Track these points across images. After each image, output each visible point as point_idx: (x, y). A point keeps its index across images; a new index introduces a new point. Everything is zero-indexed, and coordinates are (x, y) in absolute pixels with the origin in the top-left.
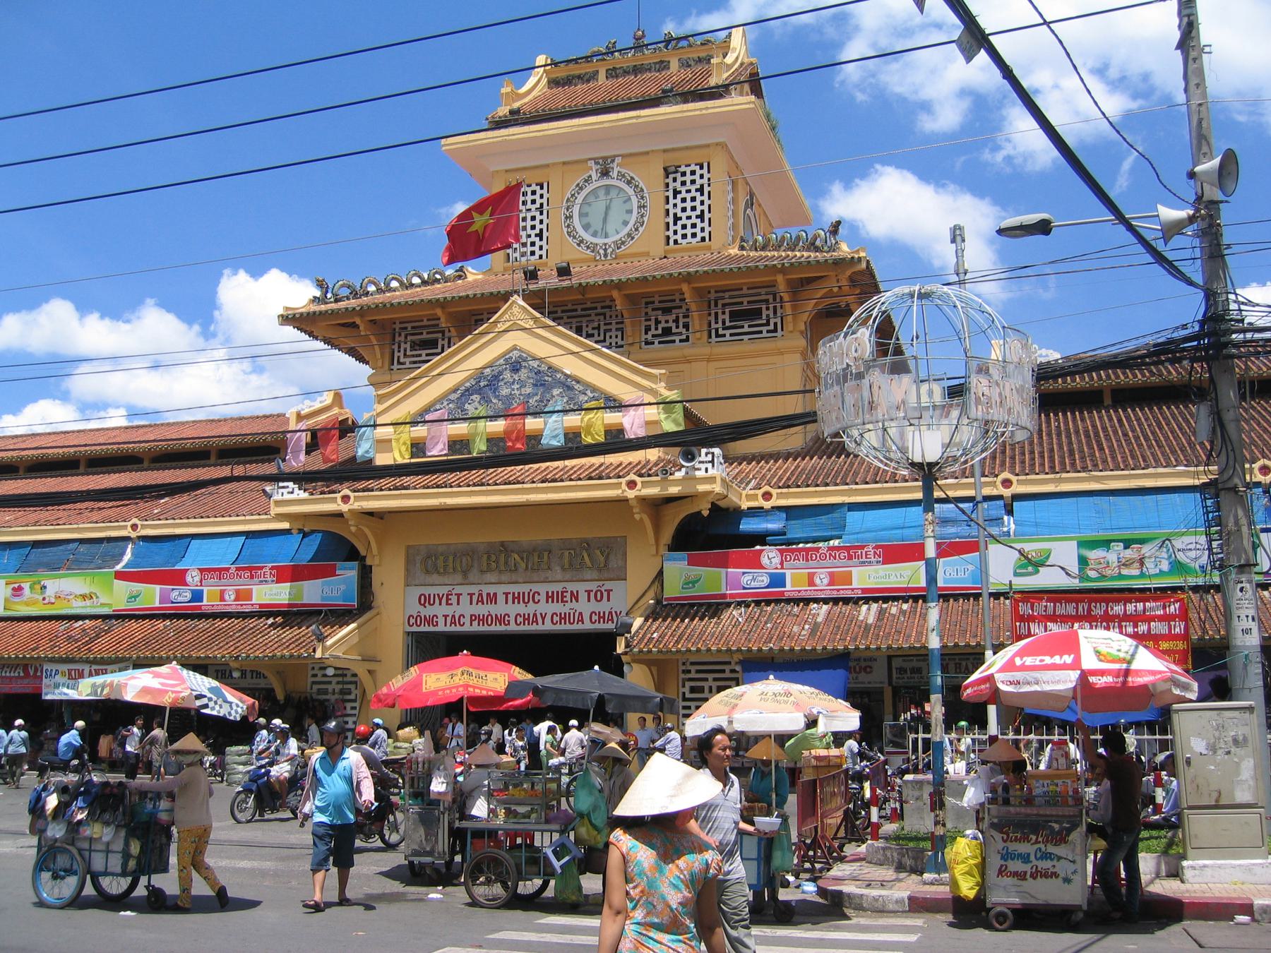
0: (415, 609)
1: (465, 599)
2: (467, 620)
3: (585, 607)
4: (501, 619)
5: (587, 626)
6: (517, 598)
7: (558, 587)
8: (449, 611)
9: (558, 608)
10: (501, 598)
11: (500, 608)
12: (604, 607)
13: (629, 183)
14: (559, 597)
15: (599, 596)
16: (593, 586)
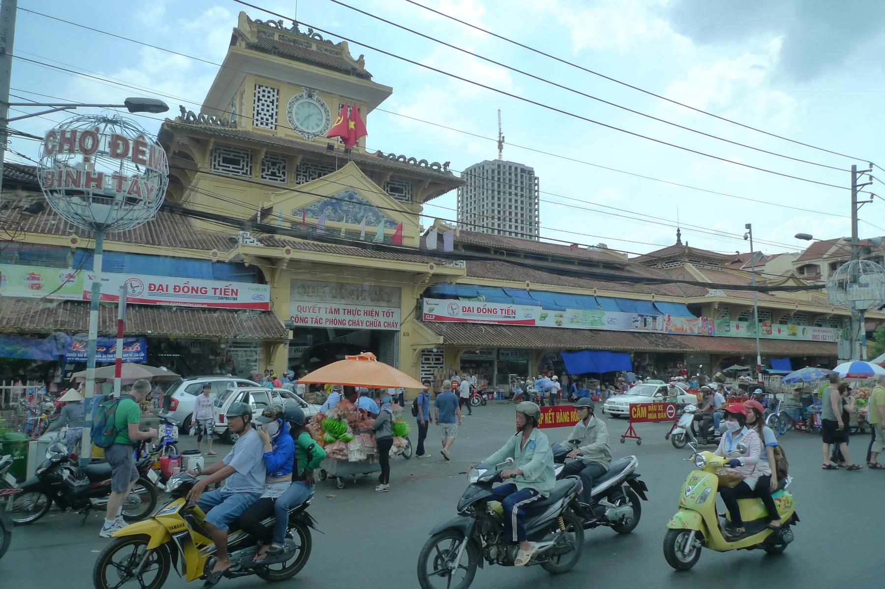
0: (295, 313)
1: (323, 311)
2: (324, 321)
3: (382, 319)
4: (341, 322)
5: (382, 328)
6: (349, 312)
7: (369, 309)
8: (314, 316)
9: (369, 318)
10: (342, 311)
11: (340, 317)
12: (390, 320)
13: (322, 105)
14: (369, 313)
15: (388, 314)
16: (385, 309)
